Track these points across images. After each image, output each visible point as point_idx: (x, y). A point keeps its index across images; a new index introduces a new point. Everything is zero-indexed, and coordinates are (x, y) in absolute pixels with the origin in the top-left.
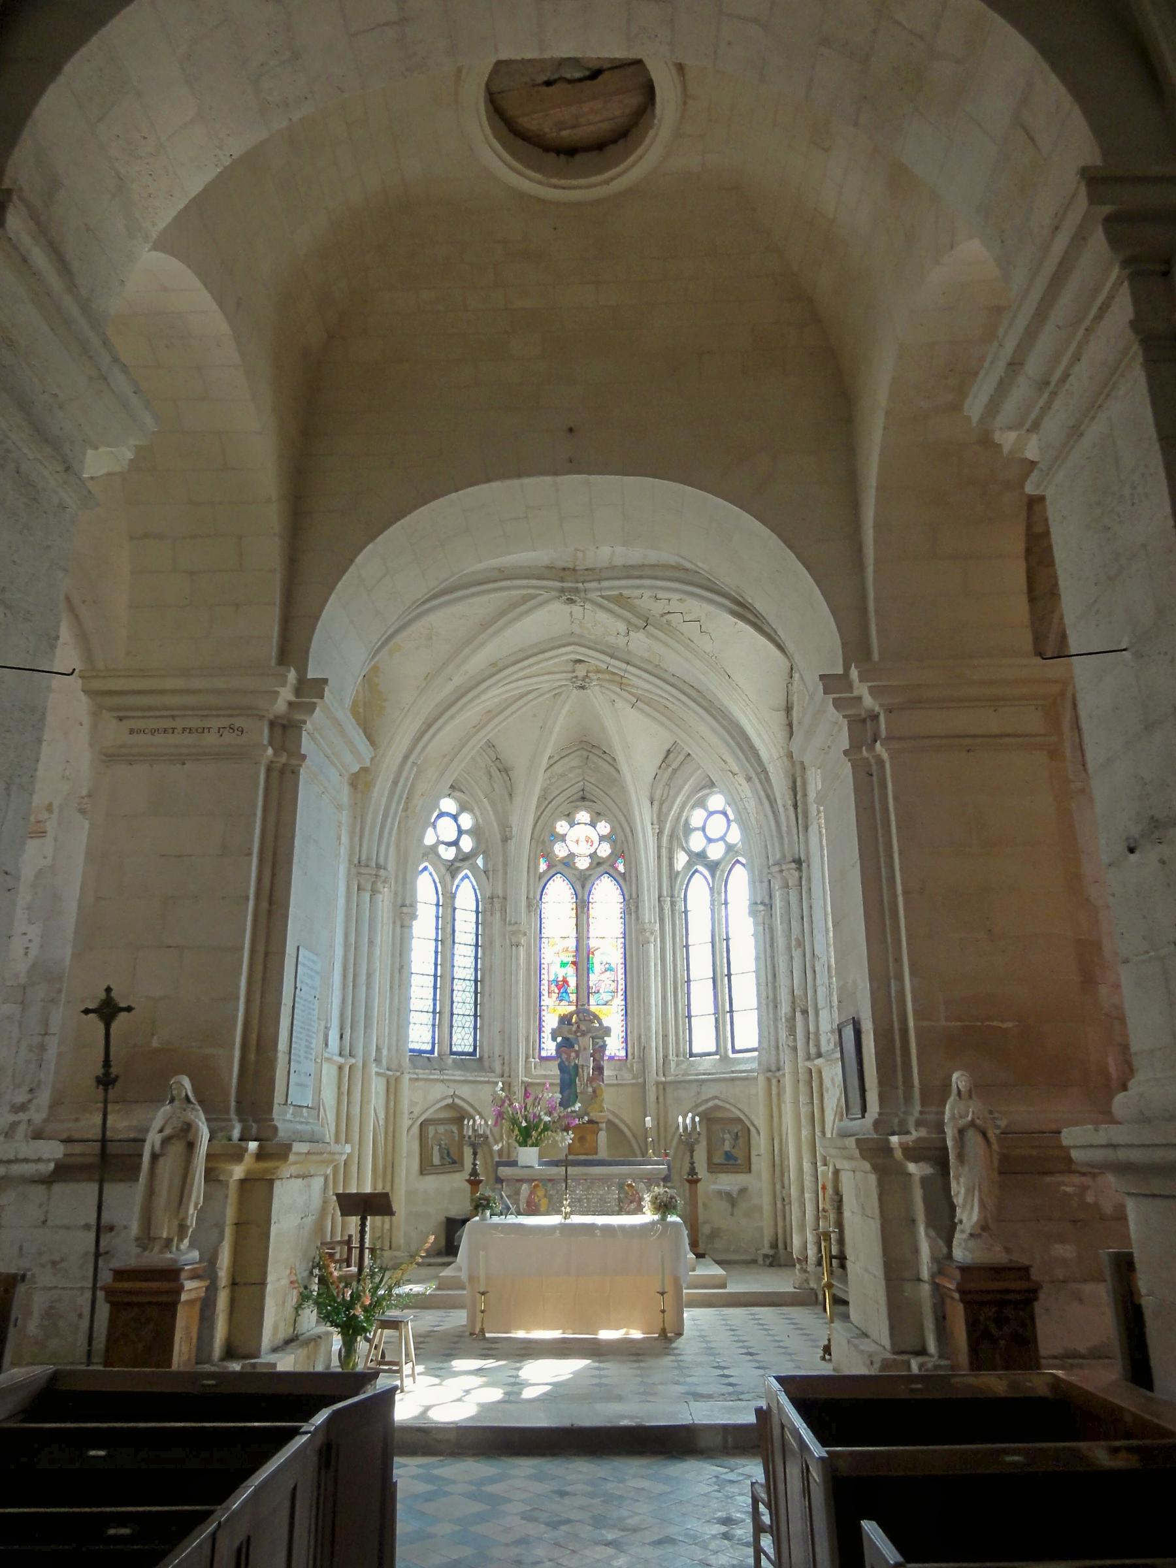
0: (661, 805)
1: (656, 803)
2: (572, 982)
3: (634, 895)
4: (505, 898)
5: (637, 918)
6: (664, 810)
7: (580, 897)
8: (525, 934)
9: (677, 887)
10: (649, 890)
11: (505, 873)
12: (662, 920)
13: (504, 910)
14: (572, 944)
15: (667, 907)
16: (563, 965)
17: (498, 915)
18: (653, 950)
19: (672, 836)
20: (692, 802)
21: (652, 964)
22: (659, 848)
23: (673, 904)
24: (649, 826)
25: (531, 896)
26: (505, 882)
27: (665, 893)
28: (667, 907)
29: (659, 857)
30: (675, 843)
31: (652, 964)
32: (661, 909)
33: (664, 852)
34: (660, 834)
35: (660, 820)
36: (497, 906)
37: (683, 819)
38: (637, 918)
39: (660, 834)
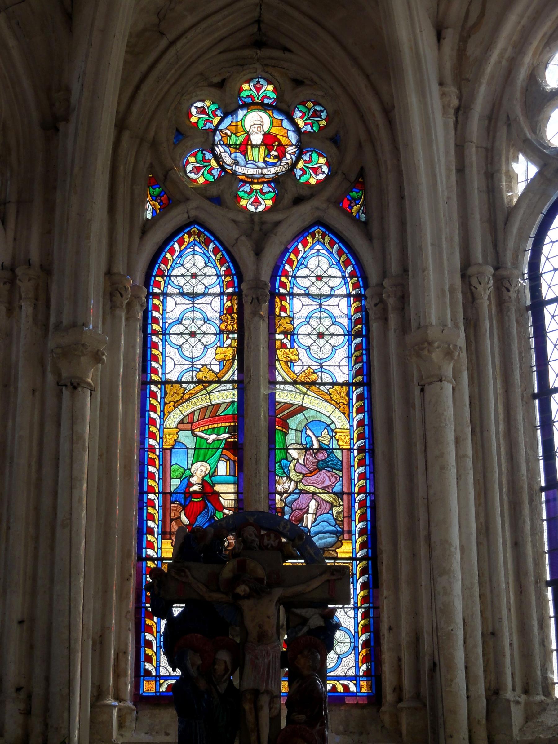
0: (464, 40)
1: (451, 37)
2: (227, 493)
3: (394, 267)
4: (47, 270)
5: (404, 327)
6: (473, 49)
7: (249, 275)
8: (97, 357)
9: (511, 244)
10: (437, 245)
11: (50, 208)
12: (472, 324)
13: (43, 300)
14: (225, 395)
15: (486, 292)
16: (202, 451)
17: (27, 309)
18: (450, 401)
19: (492, 119)
20: (546, 28)
21: (451, 436)
22: (460, 148)
23: (502, 285)
24: (435, 88)
25: (120, 267)
26: (47, 232)
27: (478, 255)
28: (486, 292)
29: (461, 170)
30: (502, 132)
31: (451, 436)
32: (471, 298)
33: (473, 156)
34: (461, 112)
35: (462, 75)
36: (25, 286)
37: (522, 74)
38: (404, 327)
39: (461, 112)
